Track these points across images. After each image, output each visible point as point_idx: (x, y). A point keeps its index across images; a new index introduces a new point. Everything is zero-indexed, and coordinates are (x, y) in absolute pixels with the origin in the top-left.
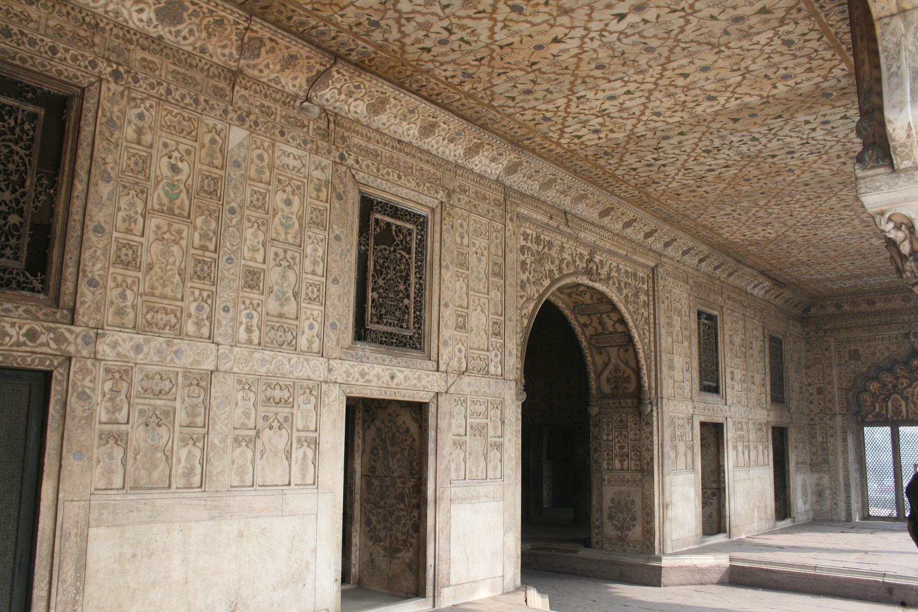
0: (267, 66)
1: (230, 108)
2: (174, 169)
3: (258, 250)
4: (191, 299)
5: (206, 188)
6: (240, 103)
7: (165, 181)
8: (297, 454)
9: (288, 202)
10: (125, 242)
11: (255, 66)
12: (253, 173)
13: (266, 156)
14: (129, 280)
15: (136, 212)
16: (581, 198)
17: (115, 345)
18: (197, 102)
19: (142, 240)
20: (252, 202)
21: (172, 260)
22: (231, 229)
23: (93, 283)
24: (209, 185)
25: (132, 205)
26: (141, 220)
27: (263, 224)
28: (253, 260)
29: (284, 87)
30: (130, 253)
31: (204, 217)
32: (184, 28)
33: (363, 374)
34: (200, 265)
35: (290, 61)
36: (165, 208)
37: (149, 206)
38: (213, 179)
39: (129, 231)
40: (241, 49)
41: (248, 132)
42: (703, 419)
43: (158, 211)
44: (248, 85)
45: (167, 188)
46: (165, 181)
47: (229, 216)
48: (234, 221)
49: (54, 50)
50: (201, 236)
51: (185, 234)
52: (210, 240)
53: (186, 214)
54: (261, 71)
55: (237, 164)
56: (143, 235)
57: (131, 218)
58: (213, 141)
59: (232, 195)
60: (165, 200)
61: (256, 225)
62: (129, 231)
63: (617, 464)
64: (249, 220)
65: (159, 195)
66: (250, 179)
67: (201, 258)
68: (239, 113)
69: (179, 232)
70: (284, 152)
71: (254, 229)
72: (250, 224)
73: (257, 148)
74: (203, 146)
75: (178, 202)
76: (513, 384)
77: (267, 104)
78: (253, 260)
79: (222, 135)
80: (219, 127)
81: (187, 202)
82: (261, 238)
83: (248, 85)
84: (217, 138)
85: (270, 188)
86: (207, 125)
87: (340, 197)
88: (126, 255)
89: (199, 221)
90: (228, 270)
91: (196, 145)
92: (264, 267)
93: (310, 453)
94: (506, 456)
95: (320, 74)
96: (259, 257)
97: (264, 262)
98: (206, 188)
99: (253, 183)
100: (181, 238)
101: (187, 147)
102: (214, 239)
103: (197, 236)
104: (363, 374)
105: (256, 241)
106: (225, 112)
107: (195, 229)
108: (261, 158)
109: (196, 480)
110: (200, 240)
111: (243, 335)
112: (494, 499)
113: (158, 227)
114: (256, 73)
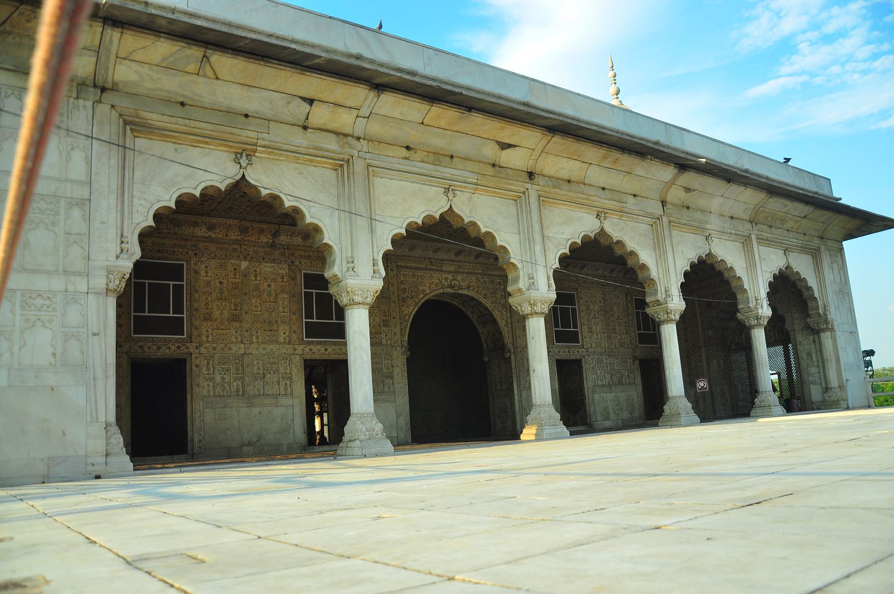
2: (221, 283)
8: (282, 383)
9: (269, 286)
16: (437, 250)
17: (206, 348)
18: (226, 256)
23: (196, 328)
25: (207, 299)
32: (217, 231)
33: (311, 350)
35: (261, 231)
40: (241, 232)
42: (558, 357)
49: (174, 252)
58: (235, 269)
63: (499, 387)
76: (399, 349)
87: (293, 279)
93: (288, 383)
94: (396, 382)
95: (275, 233)
104: (311, 350)
109: (241, 393)
111: (255, 340)
112: (389, 401)
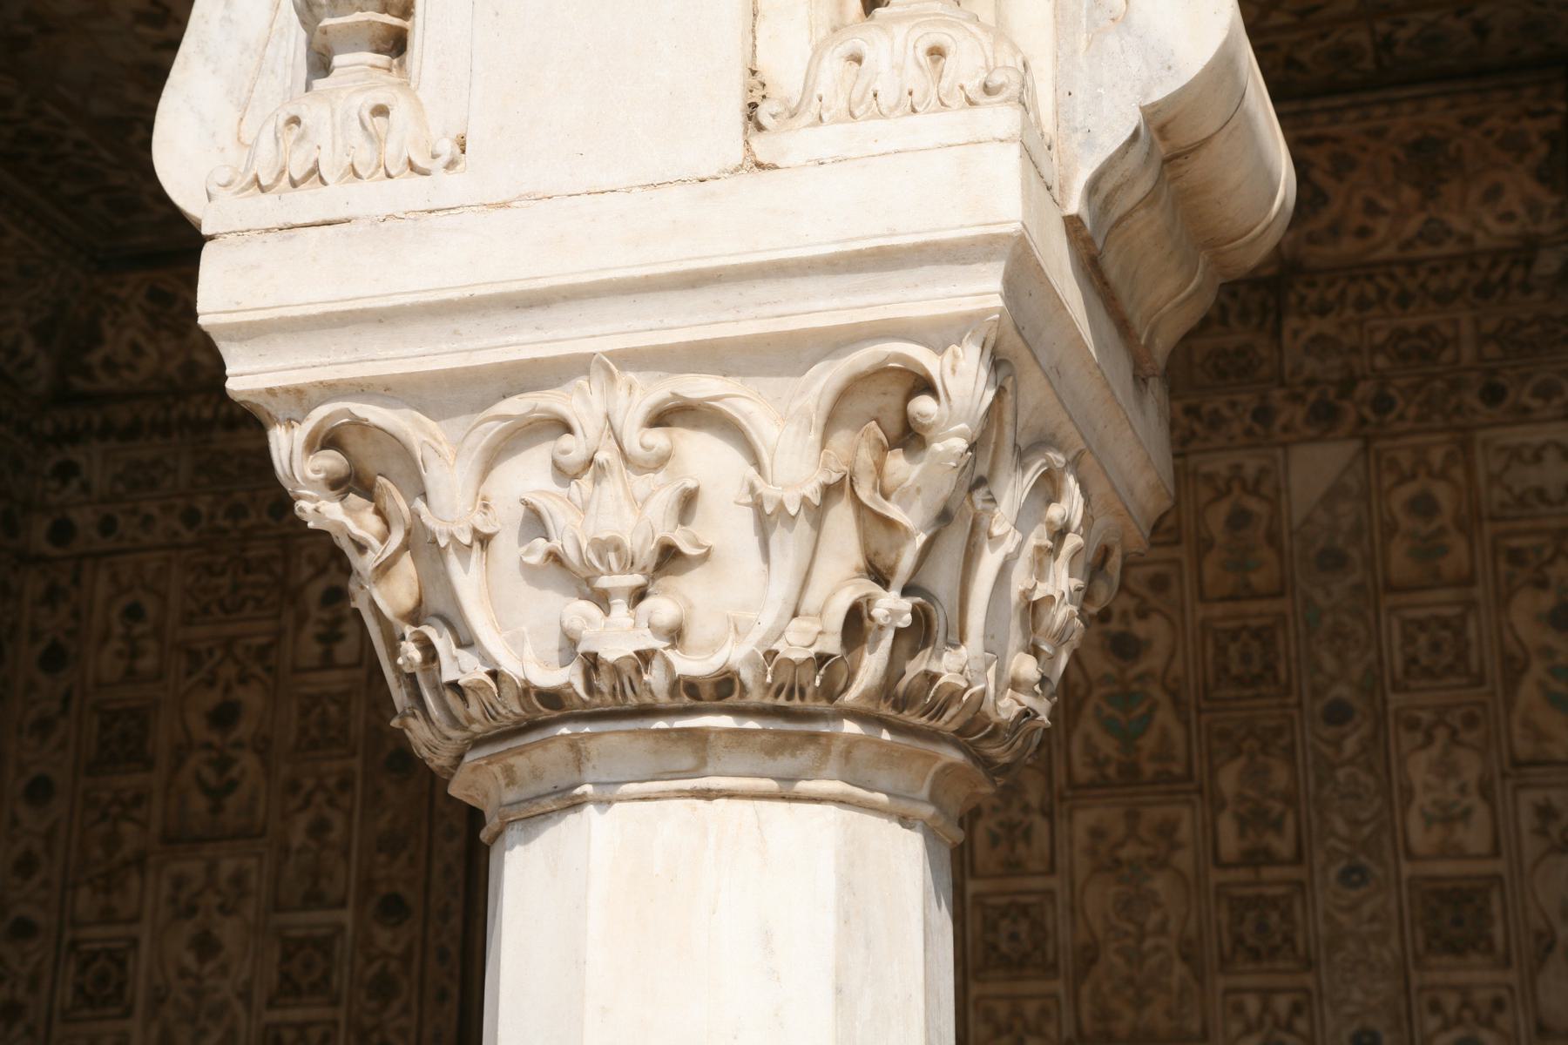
0: (1372, 208)
1: (1277, 394)
3: (1467, 814)
4: (1236, 1027)
5: (1235, 669)
6: (1311, 365)
7: (1099, 692)
10: (1003, 901)
11: (1335, 230)
12: (1400, 562)
13: (1442, 493)
14: (1031, 1009)
15: (1026, 809)
19: (1053, 883)
20: (1412, 661)
21: (1154, 918)
22: (1341, 774)
24: (1246, 658)
26: (1040, 825)
27: (1471, 721)
28: (1450, 850)
29: (1467, 239)
30: (1023, 927)
31: (1241, 762)
34: (1251, 915)
36: (1111, 771)
37: (1060, 778)
38: (1257, 634)
39: (1013, 867)
41: (1354, 446)
43: (1091, 785)
44: (1331, 295)
45: (1108, 710)
46: (1099, 692)
47: (1329, 732)
48: (1350, 745)
50: (1243, 823)
51: (1185, 832)
52: (1277, 826)
53: (1178, 769)
54: (1363, 232)
55: (1332, 561)
56: (1051, 869)
57: (1010, 827)
58: (1240, 519)
59: (1329, 663)
60: (1108, 746)
61: (1441, 734)
62: (1013, 867)
64: (1413, 725)
65: (1087, 738)
66: (1391, 588)
67: (1250, 892)
68: (1312, 396)
69: (1167, 830)
70: (1515, 453)
71: (1435, 751)
72: (1419, 737)
73: (1403, 479)
74: (1205, 545)
75: (1148, 742)
77: (1413, 322)
78: (1450, 850)
79: (1266, 489)
80: (1251, 466)
81: (1177, 733)
82: (1471, 768)
83: (1331, 295)
84: (1253, 504)
85: (1477, 592)
86: (1209, 478)
88: (1014, 937)
89: (1229, 780)
90: (1353, 908)
91: (1182, 553)
92: (1500, 866)
96: (1475, 836)
97: (1496, 853)
98: (1235, 669)
99: (1404, 599)
100: (1175, 846)
101: (1151, 570)
102: (1290, 822)
103: (1227, 826)
105: (1452, 785)
106: (1263, 414)
107: (1218, 804)
108: (1424, 506)
110: (1242, 834)
113: (1097, 833)
114: (1348, 246)
